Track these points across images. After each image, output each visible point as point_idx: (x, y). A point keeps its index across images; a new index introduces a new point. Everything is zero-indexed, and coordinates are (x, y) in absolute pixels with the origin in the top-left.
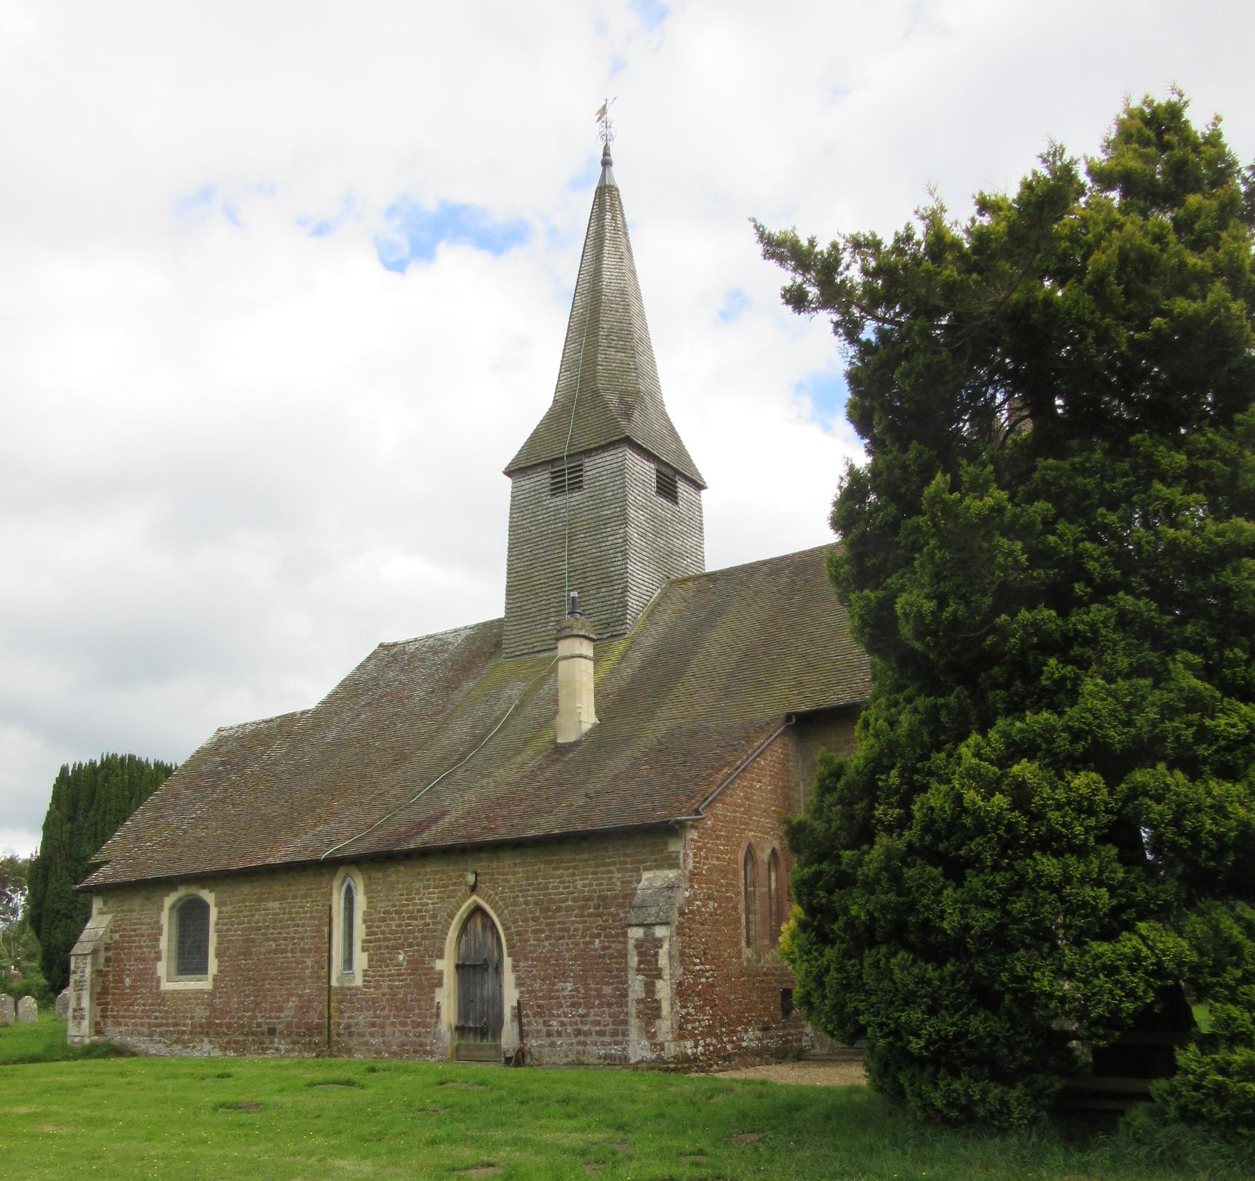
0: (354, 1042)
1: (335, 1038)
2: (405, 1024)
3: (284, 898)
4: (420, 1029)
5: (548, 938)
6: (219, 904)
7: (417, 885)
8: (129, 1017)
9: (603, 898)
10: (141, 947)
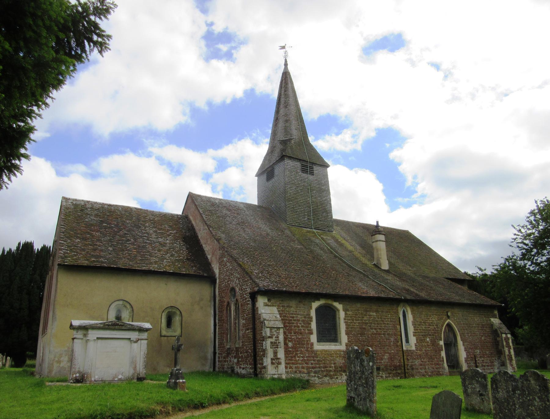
0: (415, 371)
1: (406, 371)
2: (432, 364)
3: (377, 311)
4: (437, 366)
5: (471, 336)
6: (345, 310)
7: (430, 314)
8: (293, 363)
9: (483, 325)
10: (299, 327)
